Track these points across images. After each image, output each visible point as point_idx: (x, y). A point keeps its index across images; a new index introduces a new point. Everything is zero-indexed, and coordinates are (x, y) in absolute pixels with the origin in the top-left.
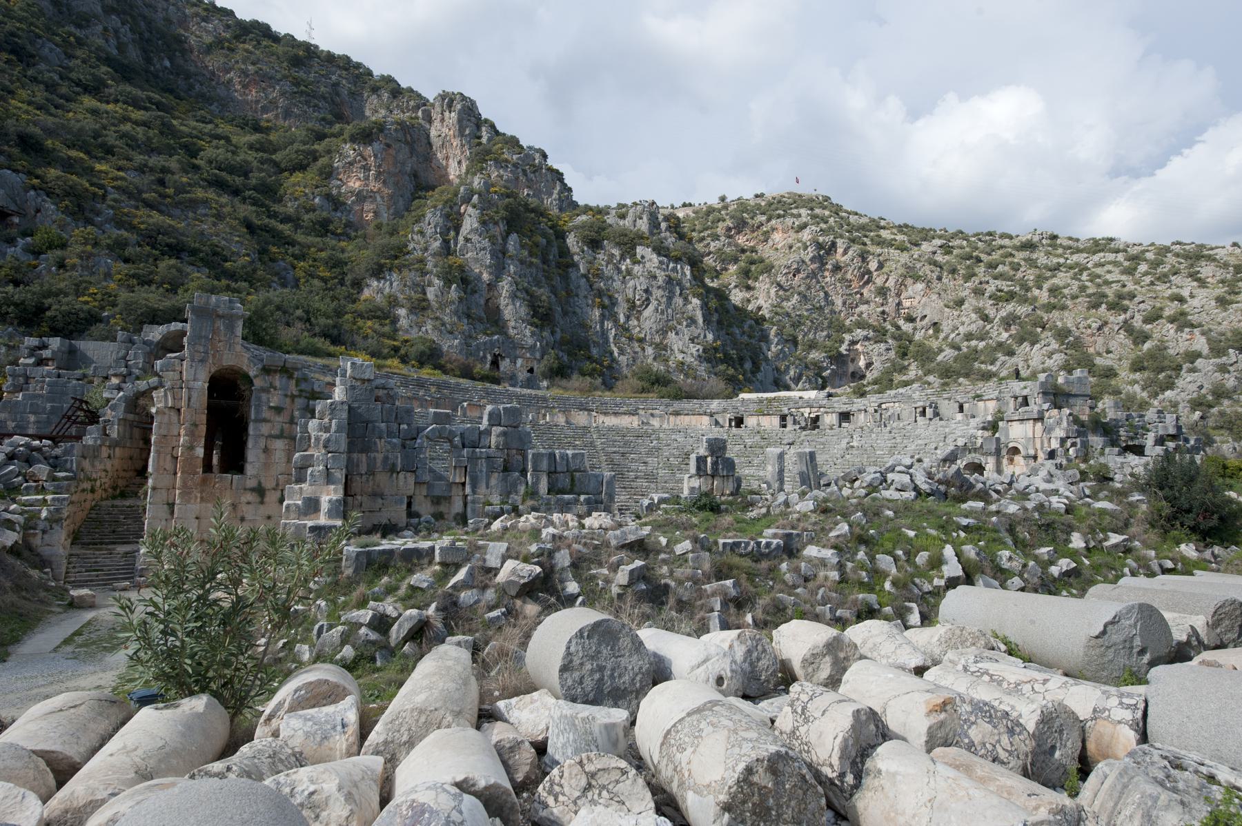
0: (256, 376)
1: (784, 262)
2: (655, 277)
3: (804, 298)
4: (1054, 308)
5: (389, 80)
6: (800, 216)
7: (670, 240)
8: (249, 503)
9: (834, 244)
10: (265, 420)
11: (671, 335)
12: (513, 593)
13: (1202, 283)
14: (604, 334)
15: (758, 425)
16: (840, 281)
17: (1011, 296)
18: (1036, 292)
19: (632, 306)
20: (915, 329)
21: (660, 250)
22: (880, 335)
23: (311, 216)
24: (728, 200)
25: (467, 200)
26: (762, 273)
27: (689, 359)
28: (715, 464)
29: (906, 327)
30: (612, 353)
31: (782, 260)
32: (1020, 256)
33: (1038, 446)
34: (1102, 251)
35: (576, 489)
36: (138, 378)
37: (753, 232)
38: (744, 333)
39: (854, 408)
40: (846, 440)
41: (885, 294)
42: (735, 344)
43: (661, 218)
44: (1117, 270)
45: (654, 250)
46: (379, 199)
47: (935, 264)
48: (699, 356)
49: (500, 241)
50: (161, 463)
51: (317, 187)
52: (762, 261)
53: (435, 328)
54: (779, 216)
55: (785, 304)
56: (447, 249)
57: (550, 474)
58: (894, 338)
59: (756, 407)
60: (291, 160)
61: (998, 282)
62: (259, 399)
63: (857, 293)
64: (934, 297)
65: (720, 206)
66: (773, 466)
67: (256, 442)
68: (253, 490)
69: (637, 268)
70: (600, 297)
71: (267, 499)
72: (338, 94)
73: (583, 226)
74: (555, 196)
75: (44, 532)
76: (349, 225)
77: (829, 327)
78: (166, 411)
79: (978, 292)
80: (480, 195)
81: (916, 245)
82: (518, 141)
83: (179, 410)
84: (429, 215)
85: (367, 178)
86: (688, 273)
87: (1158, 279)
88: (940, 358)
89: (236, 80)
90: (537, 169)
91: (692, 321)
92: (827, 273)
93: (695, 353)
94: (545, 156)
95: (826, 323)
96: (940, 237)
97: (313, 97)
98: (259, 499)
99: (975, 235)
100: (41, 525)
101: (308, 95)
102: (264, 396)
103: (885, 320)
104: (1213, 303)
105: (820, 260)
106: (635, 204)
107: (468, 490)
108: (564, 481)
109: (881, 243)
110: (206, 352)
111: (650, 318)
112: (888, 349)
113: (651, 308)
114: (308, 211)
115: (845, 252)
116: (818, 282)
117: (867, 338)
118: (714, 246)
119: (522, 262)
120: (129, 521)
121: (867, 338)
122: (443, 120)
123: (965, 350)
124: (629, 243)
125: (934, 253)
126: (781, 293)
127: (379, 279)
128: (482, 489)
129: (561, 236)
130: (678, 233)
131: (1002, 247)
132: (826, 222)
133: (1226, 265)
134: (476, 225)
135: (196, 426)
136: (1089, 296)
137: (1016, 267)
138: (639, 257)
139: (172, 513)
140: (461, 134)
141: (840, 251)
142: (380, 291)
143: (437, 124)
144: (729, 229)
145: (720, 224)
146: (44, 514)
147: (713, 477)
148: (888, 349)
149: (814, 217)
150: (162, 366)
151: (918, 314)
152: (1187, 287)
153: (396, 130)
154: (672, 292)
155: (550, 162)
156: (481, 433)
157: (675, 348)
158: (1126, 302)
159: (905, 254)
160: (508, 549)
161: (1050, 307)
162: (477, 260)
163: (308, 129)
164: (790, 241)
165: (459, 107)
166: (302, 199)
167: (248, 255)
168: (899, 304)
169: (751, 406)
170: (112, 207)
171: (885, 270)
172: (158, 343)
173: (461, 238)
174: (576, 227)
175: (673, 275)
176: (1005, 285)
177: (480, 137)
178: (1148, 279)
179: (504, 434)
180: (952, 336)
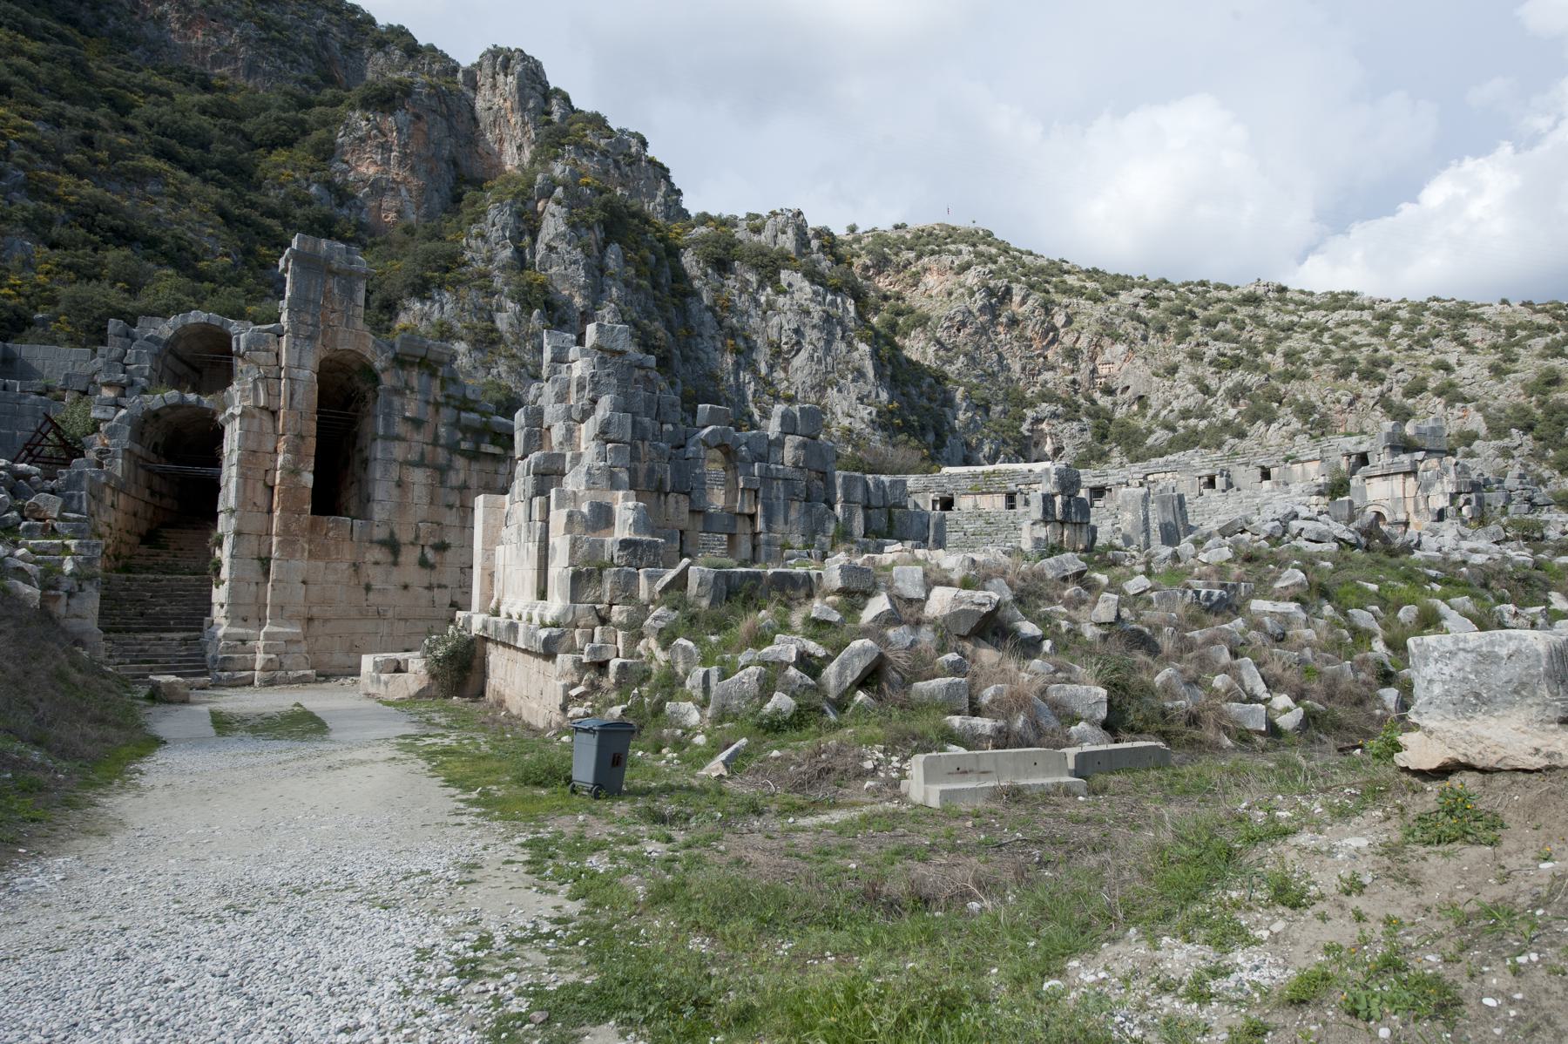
0: (384, 370)
1: (943, 312)
2: (808, 313)
3: (972, 360)
4: (1293, 377)
5: (400, 33)
6: (960, 252)
7: (825, 264)
8: (376, 563)
9: (1008, 291)
10: (398, 438)
11: (832, 393)
12: (964, 630)
13: (1470, 348)
14: (740, 389)
15: (975, 506)
16: (1018, 339)
17: (1237, 362)
18: (1268, 357)
19: (777, 352)
20: (1115, 404)
21: (812, 275)
22: (1071, 411)
23: (306, 210)
24: (860, 231)
25: (547, 194)
26: (914, 327)
27: (858, 426)
28: (1066, 505)
29: (1104, 401)
30: (751, 416)
31: (938, 310)
32: (1243, 312)
33: (1411, 508)
34: (1343, 307)
35: (896, 533)
36: (144, 391)
37: (898, 272)
38: (922, 394)
39: (1111, 481)
40: (1110, 522)
41: (1076, 358)
42: (913, 409)
43: (810, 234)
44: (1365, 331)
45: (805, 275)
46: (404, 192)
47: (1139, 319)
48: (872, 421)
49: (596, 253)
50: (249, 494)
51: (313, 170)
52: (911, 311)
53: (511, 370)
54: (933, 253)
56: (521, 262)
57: (866, 507)
58: (1089, 415)
59: (970, 484)
60: (268, 131)
61: (1219, 344)
62: (389, 404)
63: (1039, 356)
64: (1139, 362)
65: (850, 237)
66: (1135, 512)
67: (386, 470)
68: (382, 543)
69: (781, 300)
70: (733, 337)
71: (401, 559)
72: (325, 47)
73: (704, 240)
74: (659, 199)
75: (70, 595)
76: (360, 226)
78: (256, 411)
79: (1195, 357)
80: (565, 187)
81: (1113, 295)
82: (604, 121)
83: (274, 414)
84: (492, 213)
85: (386, 162)
86: (852, 308)
87: (1418, 342)
88: (1150, 441)
89: (173, 15)
90: (634, 160)
91: (860, 374)
92: (1000, 329)
93: (867, 417)
94: (644, 143)
96: (1141, 286)
97: (291, 48)
98: (390, 559)
99: (1184, 285)
100: (66, 584)
101: (283, 44)
102: (397, 401)
103: (1076, 392)
104: (1486, 372)
105: (992, 311)
106: (774, 214)
107: (760, 524)
108: (881, 521)
109: (1068, 291)
110: (316, 326)
111: (802, 368)
112: (1082, 430)
113: (803, 355)
114: (300, 204)
115: (1023, 302)
116: (989, 340)
117: (1054, 415)
119: (627, 284)
120: (162, 601)
121: (1054, 415)
122: (494, 87)
123: (1181, 431)
124: (769, 266)
125: (1136, 305)
126: (941, 353)
127: (423, 299)
128: (779, 526)
129: (674, 252)
130: (834, 255)
131: (1219, 300)
132: (995, 262)
133: (1495, 327)
134: (563, 228)
135: (303, 438)
136: (1336, 362)
137: (1240, 326)
138: (784, 284)
139: (267, 573)
140: (523, 107)
141: (1017, 299)
142: (425, 316)
143: (485, 91)
144: (866, 268)
146: (68, 566)
147: (1062, 523)
148: (1082, 430)
149: (979, 255)
150: (249, 342)
151: (1118, 384)
152: (1453, 354)
153: (429, 95)
154: (831, 334)
155: (650, 152)
156: (771, 443)
157: (838, 409)
158: (1381, 370)
159: (1099, 306)
160: (925, 575)
161: (1288, 377)
162: (565, 278)
163: (286, 93)
164: (948, 285)
165: (519, 68)
166: (292, 187)
167: (227, 255)
168: (1094, 371)
169: (962, 482)
170: (23, 168)
171: (1075, 325)
172: (168, 342)
173: (541, 247)
174: (695, 242)
175: (832, 311)
176: (1228, 348)
177: (549, 113)
178: (1405, 343)
179: (803, 446)
180: (1164, 413)
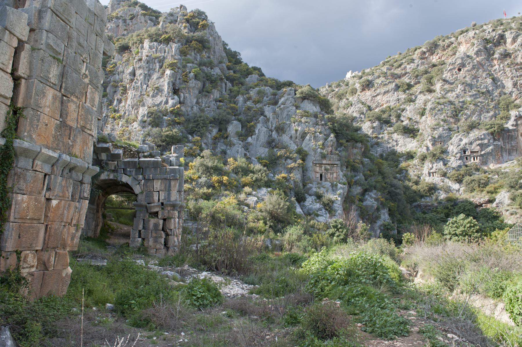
9: (502, 37)
16: (509, 66)
37: (444, 50)
55: (449, 94)
77: (495, 107)
91: (159, 90)
95: (492, 105)
115: (514, 40)
118: (410, 67)
126: (447, 86)
141: (509, 41)
144: (424, 53)
145: (418, 51)
